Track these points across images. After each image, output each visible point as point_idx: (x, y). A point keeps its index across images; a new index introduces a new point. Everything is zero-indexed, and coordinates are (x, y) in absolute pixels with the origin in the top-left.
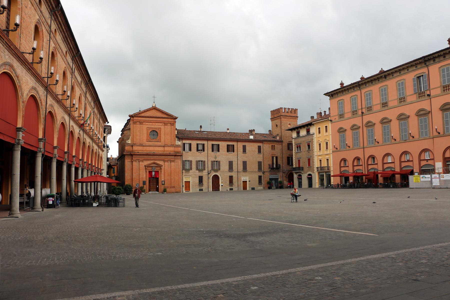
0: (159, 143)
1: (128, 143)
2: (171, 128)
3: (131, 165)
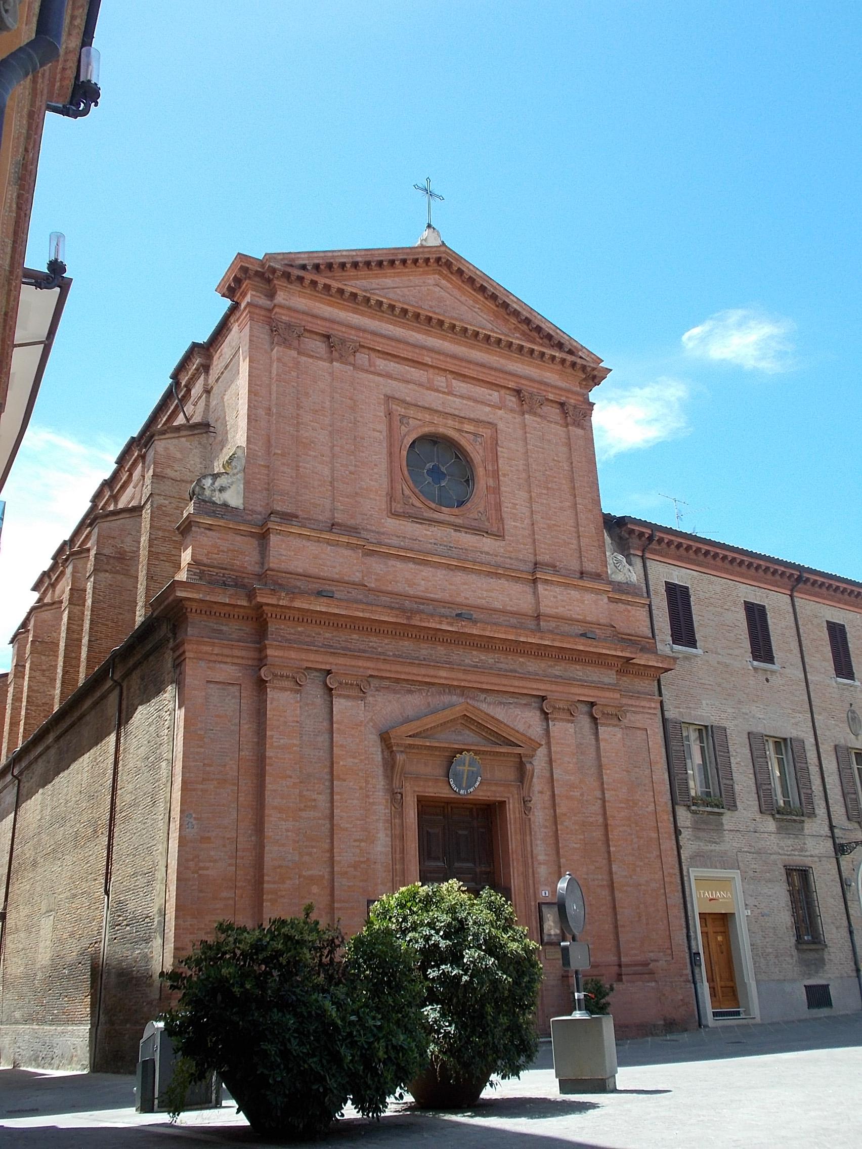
0: (487, 543)
1: (218, 498)
2: (569, 445)
3: (247, 727)
